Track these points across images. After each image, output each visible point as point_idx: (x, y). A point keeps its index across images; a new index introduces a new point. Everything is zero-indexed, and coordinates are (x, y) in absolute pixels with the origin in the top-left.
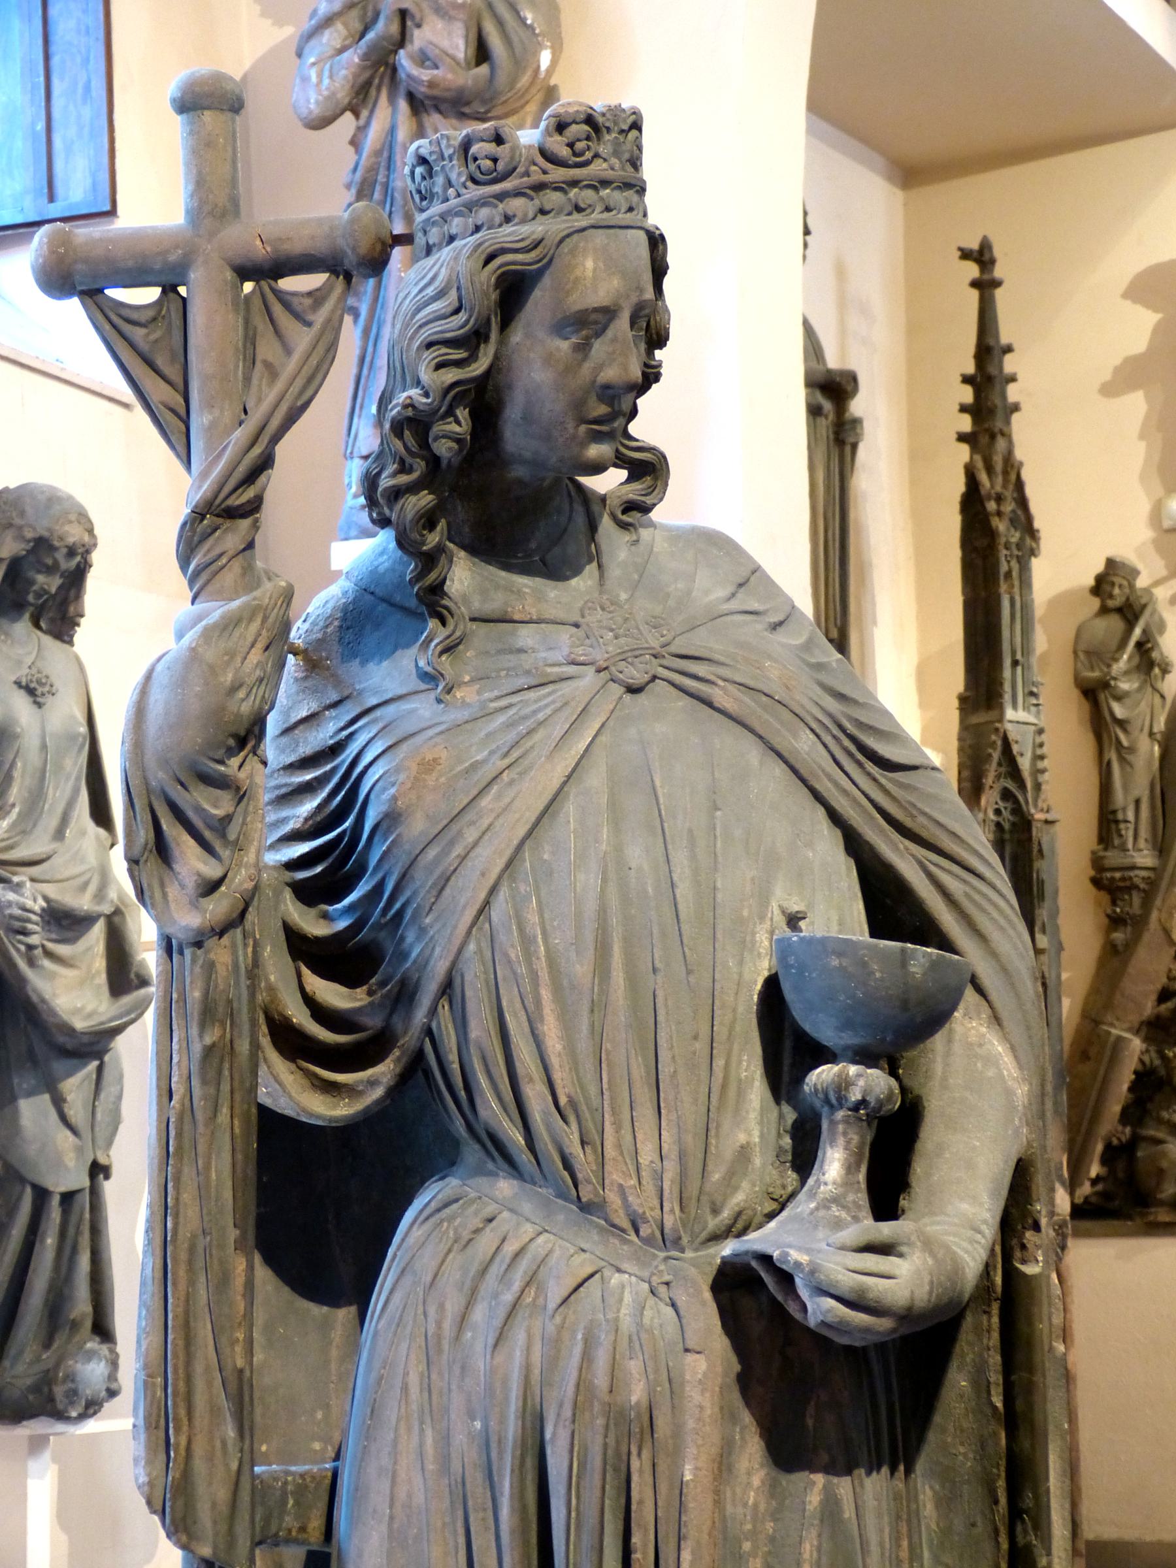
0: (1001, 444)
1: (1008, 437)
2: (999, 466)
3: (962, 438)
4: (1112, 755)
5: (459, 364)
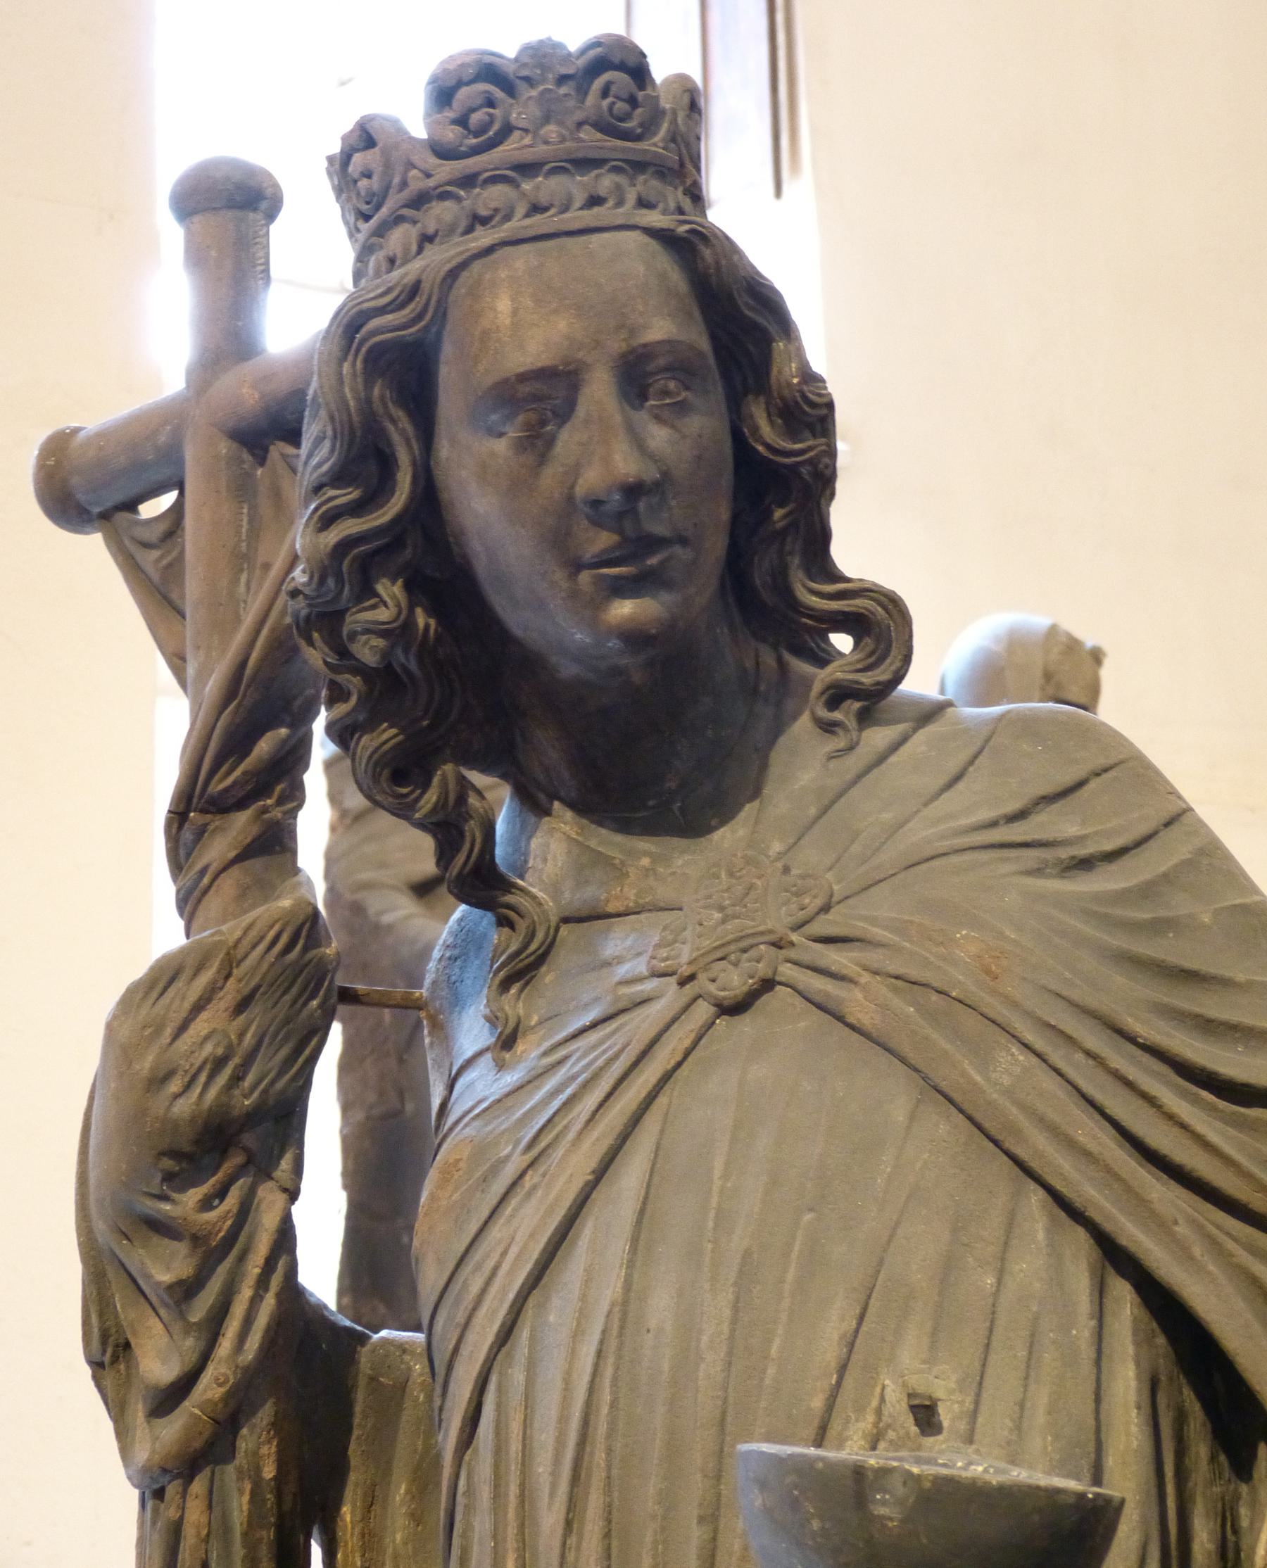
5: (357, 509)
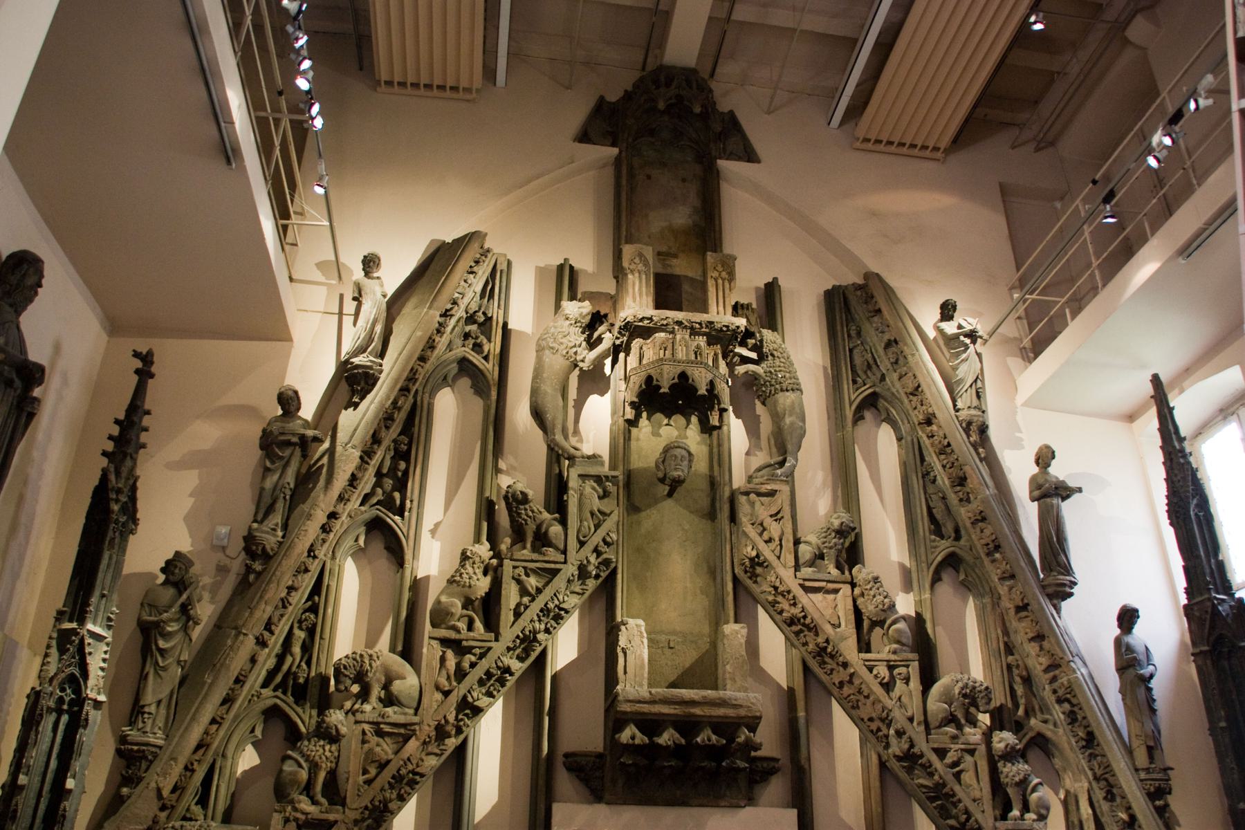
0: (128, 463)
1: (134, 460)
2: (124, 475)
3: (104, 454)
4: (149, 668)
